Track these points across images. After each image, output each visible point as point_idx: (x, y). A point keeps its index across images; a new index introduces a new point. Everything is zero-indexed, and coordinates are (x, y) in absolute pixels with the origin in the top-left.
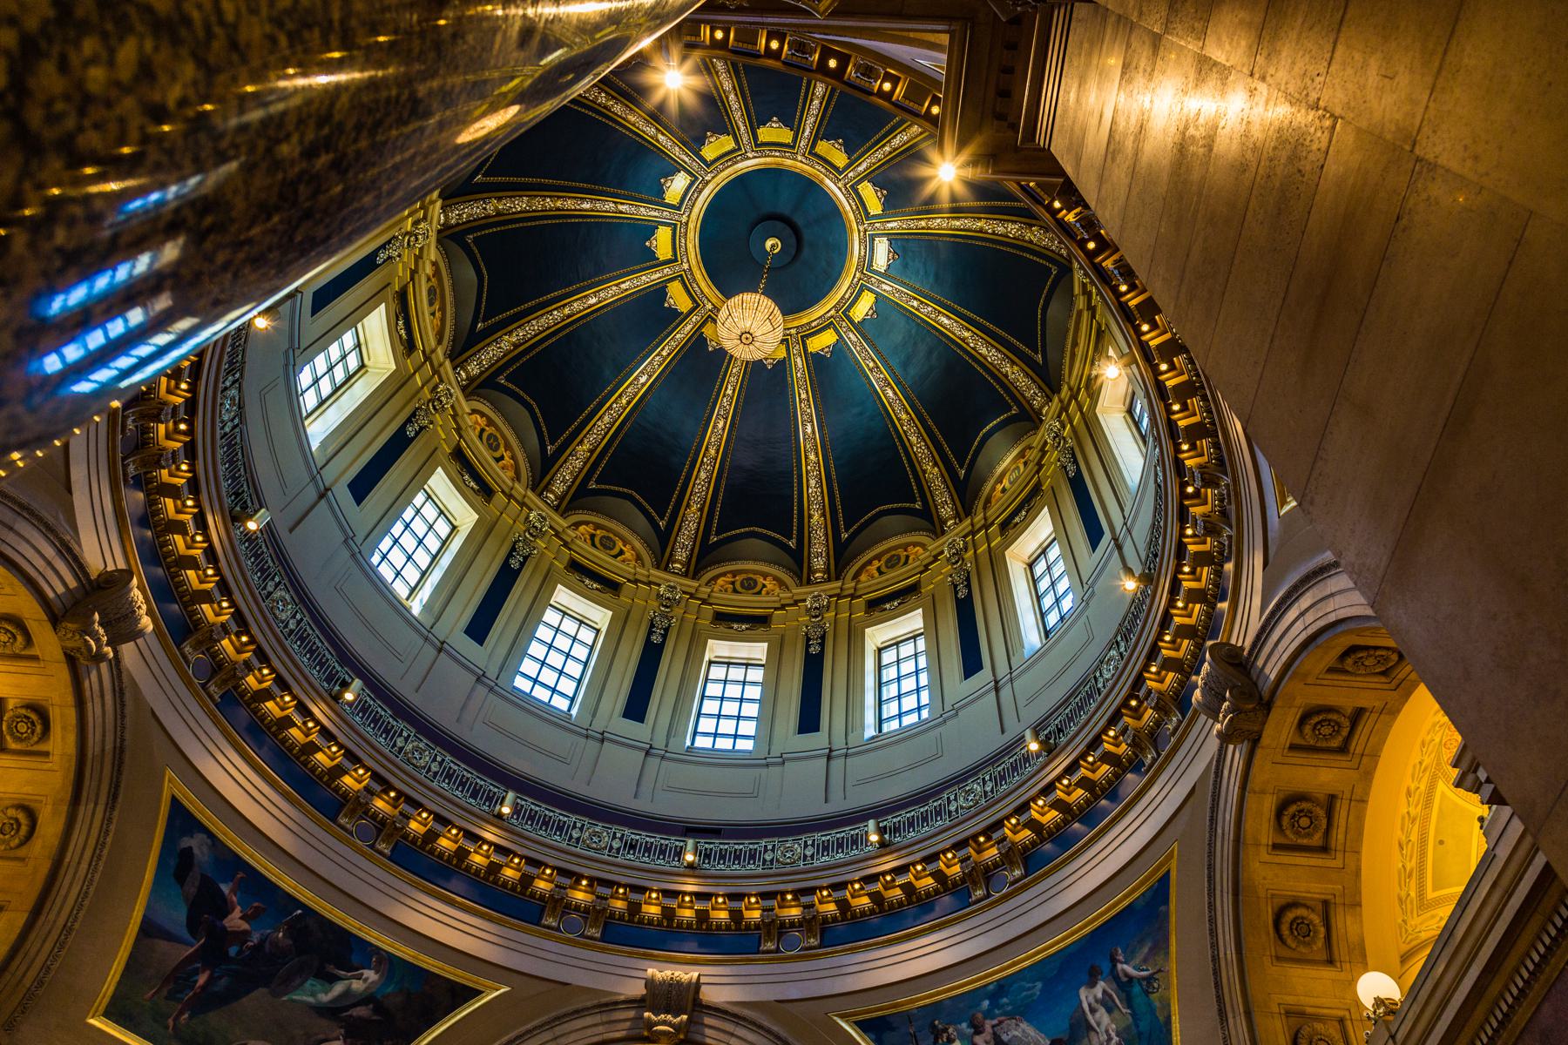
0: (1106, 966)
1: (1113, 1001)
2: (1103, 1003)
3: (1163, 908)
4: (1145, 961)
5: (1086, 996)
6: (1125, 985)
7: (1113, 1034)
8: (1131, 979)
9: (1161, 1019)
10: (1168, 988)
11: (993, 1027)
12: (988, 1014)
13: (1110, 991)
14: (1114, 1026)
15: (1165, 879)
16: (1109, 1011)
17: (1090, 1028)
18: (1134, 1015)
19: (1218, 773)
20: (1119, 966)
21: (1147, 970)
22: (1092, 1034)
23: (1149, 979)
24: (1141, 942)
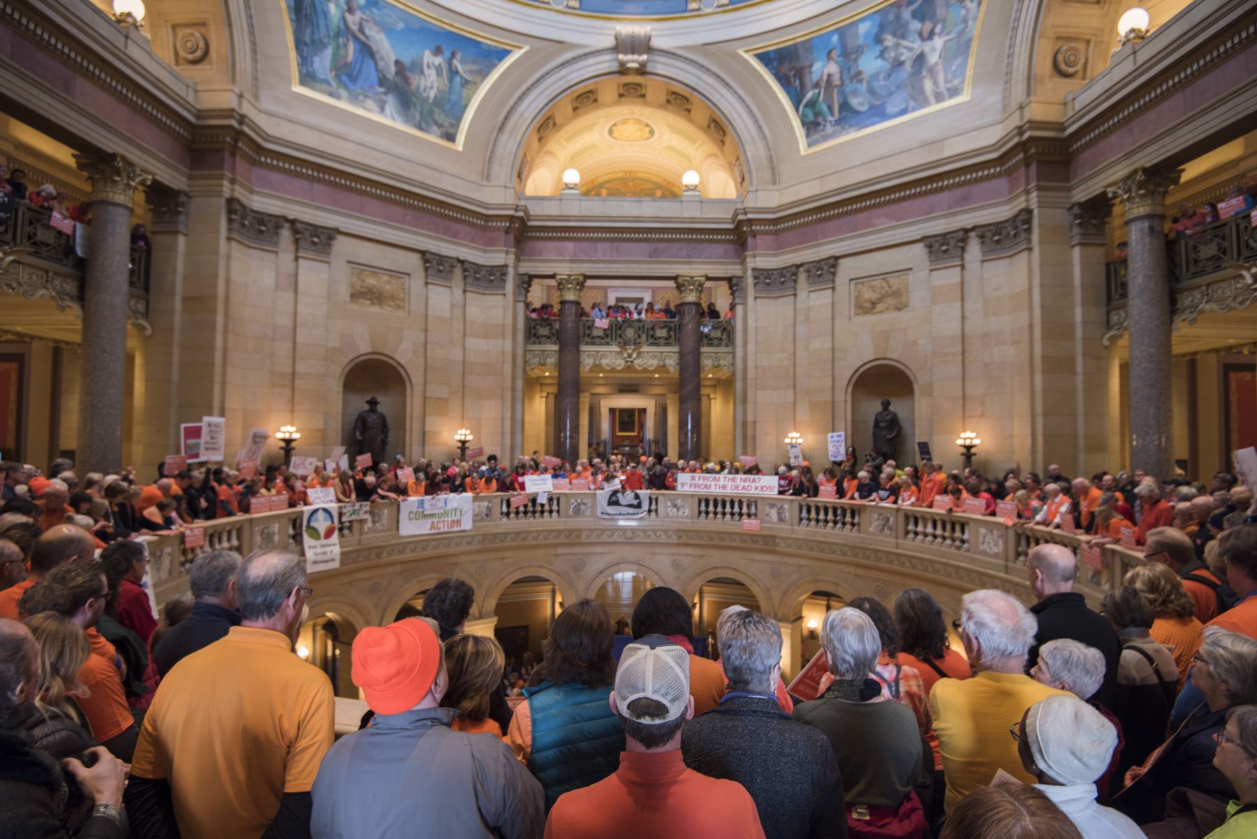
0: (447, 54)
3: (495, 61)
4: (471, 72)
5: (428, 57)
6: (453, 72)
8: (457, 72)
10: (474, 93)
11: (362, 19)
12: (361, 8)
17: (422, 72)
18: (450, 88)
19: (587, 55)
23: (467, 82)
24: (474, 62)
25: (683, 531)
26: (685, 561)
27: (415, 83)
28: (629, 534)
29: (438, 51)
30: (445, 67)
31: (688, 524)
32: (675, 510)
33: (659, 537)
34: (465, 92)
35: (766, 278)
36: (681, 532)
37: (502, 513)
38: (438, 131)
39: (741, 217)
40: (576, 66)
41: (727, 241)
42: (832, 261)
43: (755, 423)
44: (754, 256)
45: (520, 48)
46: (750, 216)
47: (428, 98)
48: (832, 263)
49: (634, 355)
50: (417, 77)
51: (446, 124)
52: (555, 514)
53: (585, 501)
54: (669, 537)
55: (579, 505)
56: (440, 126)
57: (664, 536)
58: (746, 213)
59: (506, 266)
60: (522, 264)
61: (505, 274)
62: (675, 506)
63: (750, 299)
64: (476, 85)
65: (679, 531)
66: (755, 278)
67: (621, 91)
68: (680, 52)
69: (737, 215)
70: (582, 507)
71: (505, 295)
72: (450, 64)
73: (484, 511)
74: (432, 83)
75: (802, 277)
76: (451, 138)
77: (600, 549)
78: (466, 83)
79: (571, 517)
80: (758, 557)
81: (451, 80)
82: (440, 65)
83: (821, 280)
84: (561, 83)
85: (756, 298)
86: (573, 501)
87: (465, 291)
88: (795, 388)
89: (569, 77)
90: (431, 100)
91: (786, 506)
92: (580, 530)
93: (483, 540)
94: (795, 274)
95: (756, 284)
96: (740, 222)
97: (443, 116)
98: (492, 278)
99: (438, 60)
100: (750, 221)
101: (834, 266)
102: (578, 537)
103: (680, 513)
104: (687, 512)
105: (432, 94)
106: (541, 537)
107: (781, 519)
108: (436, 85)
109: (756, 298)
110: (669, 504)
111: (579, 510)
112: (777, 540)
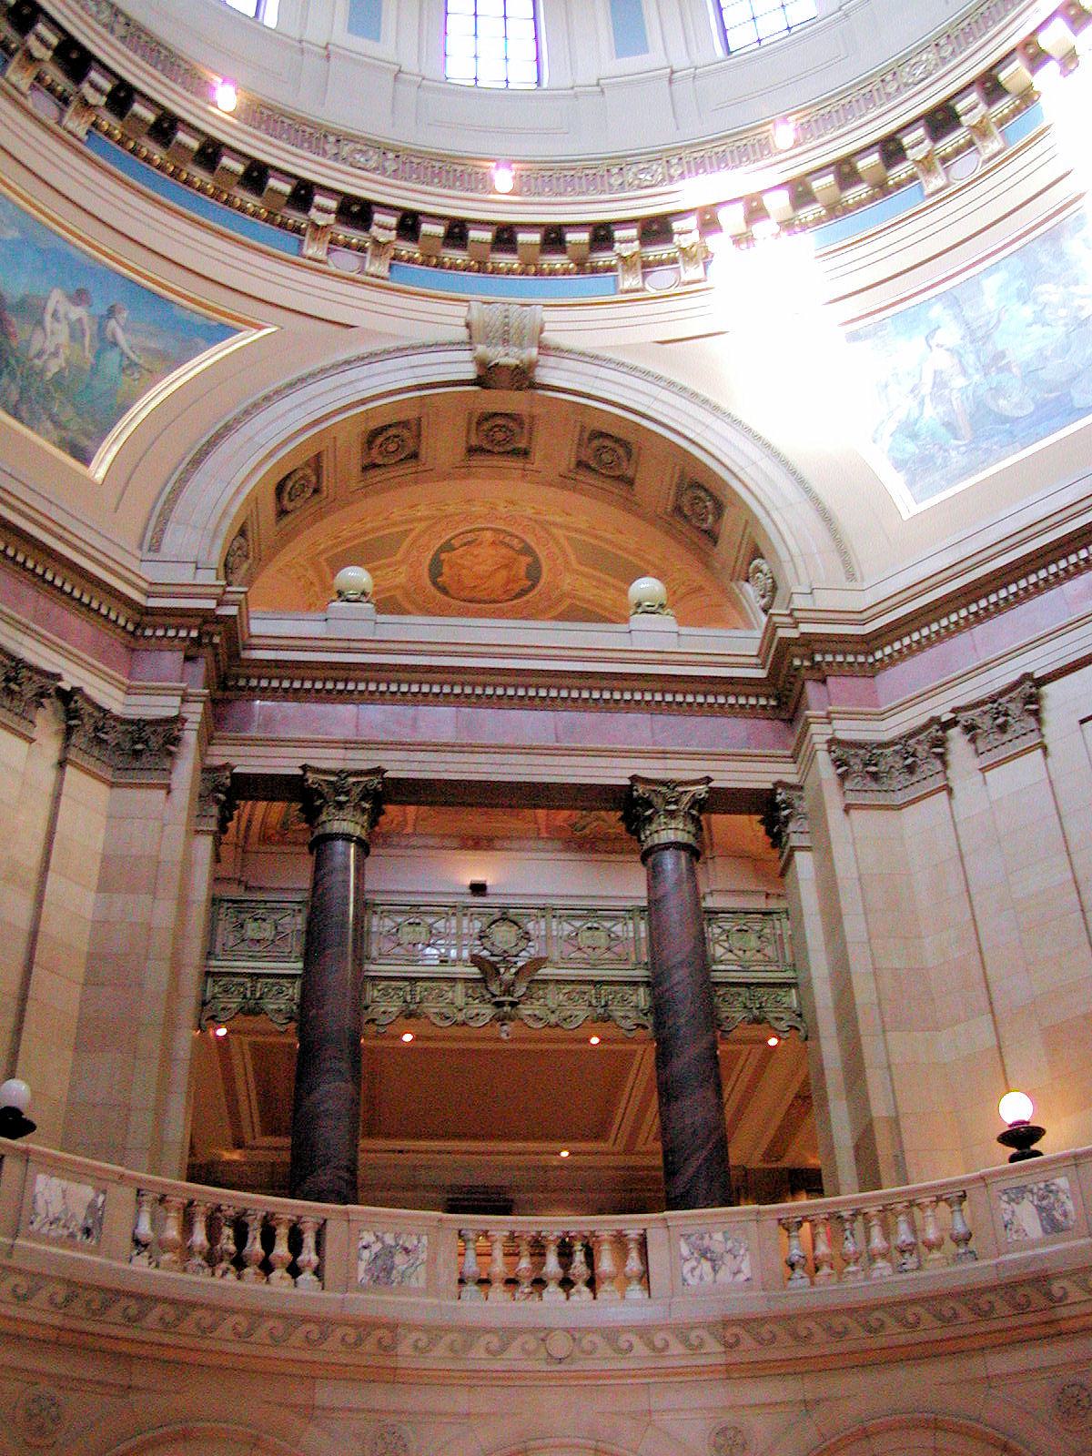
0: (101, 308)
1: (83, 335)
2: (71, 326)
3: (202, 343)
5: (57, 300)
7: (62, 356)
8: (115, 344)
9: (119, 400)
13: (86, 327)
14: (68, 352)
15: (225, 332)
16: (72, 337)
17: (40, 323)
19: (402, 351)
20: (112, 323)
21: (139, 357)
22: (39, 333)
23: (133, 364)
25: (745, 1322)
26: (760, 1427)
27: (22, 336)
28: (560, 1345)
29: (80, 297)
30: (90, 328)
31: (756, 1304)
32: (706, 1266)
33: (660, 1351)
34: (125, 382)
35: (866, 765)
36: (732, 1328)
37: (137, 1242)
38: (55, 435)
39: (781, 633)
40: (377, 367)
41: (754, 712)
42: (1027, 688)
43: (895, 1122)
44: (829, 718)
45: (260, 328)
46: (805, 628)
47: (43, 371)
48: (1030, 691)
49: (521, 989)
50: (28, 328)
51: (73, 426)
52: (307, 1276)
53: (410, 1242)
54: (695, 1349)
55: (389, 1252)
56: (58, 424)
57: (676, 1348)
58: (795, 625)
59: (179, 720)
60: (215, 749)
61: (176, 740)
62: (705, 1253)
63: (834, 813)
64: (154, 377)
65: (727, 1323)
66: (839, 762)
67: (474, 441)
68: (609, 355)
69: (775, 629)
70: (399, 1259)
71: (168, 789)
72: (101, 329)
73: (80, 1217)
74: (58, 347)
75: (957, 740)
76: (84, 457)
77: (460, 1400)
78: (129, 366)
79: (362, 1288)
80: (1001, 1363)
81: (98, 354)
82: (80, 320)
83: (1006, 737)
84: (345, 391)
85: (847, 808)
86: (368, 1237)
87: (62, 764)
88: (992, 1012)
89: (363, 385)
90: (49, 375)
91: (1062, 1182)
92: (393, 1327)
93: (68, 1300)
94: (940, 742)
95: (843, 777)
96: (786, 643)
97: (70, 411)
98: (139, 747)
99: (77, 312)
100: (809, 642)
101: (1034, 699)
102: (387, 1349)
103: (724, 1275)
104: (746, 1270)
105: (54, 367)
106: (261, 1333)
107: (1053, 1226)
108: (64, 353)
109: (847, 808)
110: (685, 1250)
111: (388, 1270)
112: (1056, 1288)
